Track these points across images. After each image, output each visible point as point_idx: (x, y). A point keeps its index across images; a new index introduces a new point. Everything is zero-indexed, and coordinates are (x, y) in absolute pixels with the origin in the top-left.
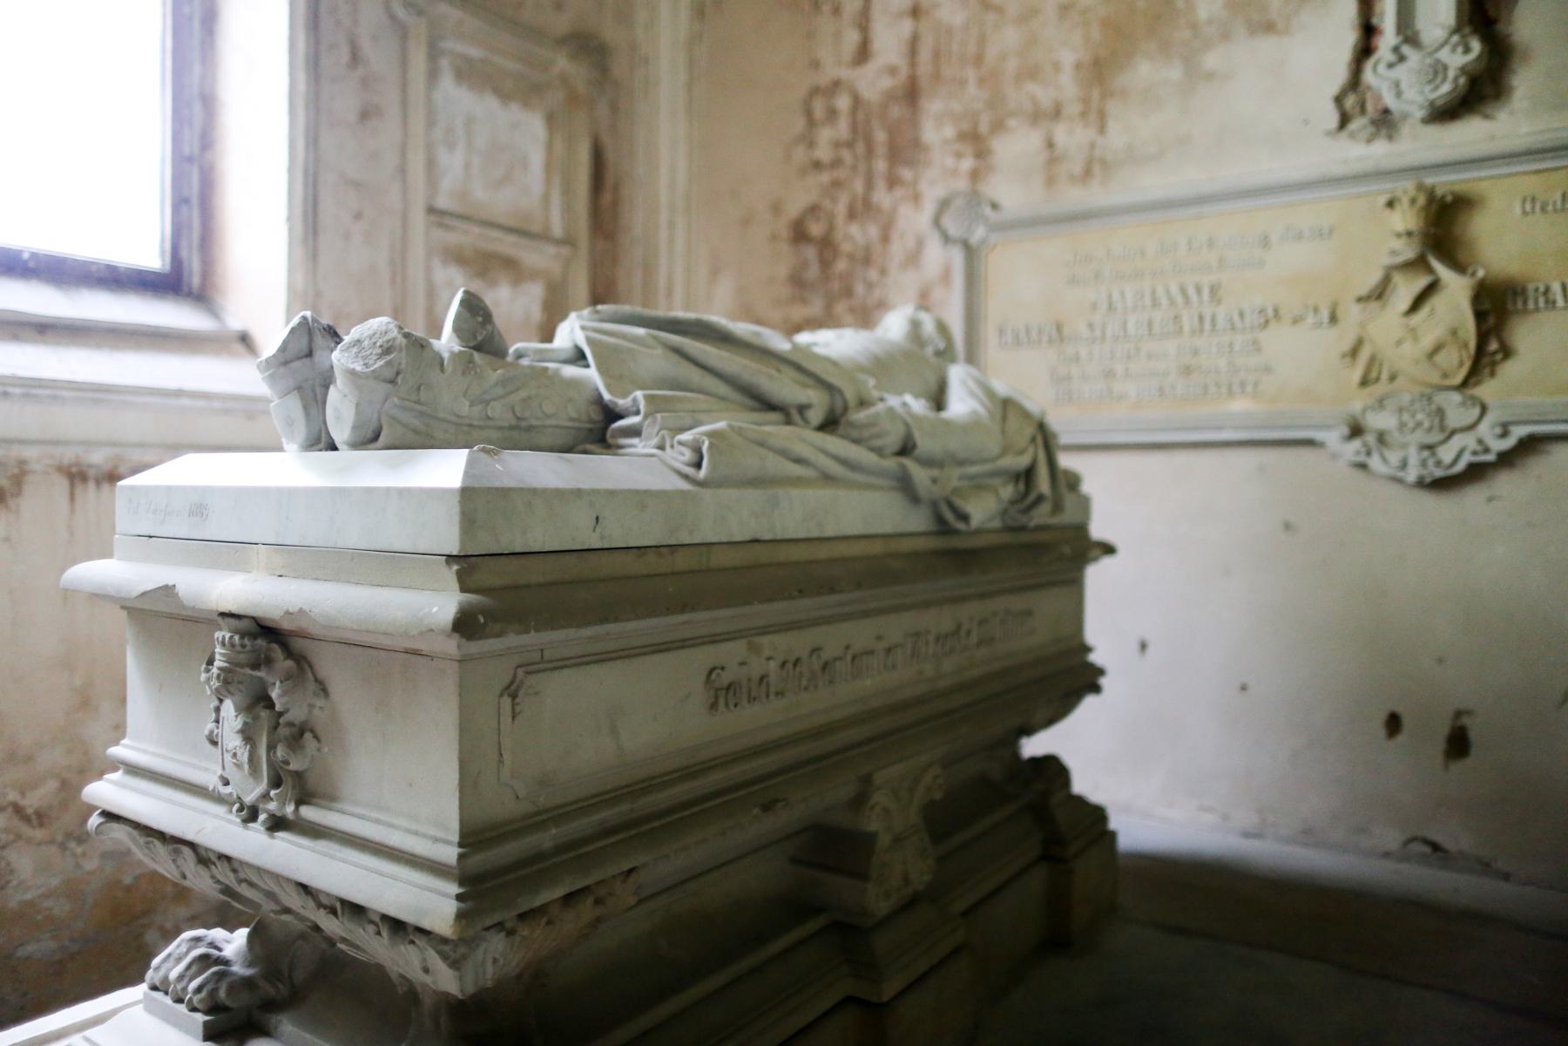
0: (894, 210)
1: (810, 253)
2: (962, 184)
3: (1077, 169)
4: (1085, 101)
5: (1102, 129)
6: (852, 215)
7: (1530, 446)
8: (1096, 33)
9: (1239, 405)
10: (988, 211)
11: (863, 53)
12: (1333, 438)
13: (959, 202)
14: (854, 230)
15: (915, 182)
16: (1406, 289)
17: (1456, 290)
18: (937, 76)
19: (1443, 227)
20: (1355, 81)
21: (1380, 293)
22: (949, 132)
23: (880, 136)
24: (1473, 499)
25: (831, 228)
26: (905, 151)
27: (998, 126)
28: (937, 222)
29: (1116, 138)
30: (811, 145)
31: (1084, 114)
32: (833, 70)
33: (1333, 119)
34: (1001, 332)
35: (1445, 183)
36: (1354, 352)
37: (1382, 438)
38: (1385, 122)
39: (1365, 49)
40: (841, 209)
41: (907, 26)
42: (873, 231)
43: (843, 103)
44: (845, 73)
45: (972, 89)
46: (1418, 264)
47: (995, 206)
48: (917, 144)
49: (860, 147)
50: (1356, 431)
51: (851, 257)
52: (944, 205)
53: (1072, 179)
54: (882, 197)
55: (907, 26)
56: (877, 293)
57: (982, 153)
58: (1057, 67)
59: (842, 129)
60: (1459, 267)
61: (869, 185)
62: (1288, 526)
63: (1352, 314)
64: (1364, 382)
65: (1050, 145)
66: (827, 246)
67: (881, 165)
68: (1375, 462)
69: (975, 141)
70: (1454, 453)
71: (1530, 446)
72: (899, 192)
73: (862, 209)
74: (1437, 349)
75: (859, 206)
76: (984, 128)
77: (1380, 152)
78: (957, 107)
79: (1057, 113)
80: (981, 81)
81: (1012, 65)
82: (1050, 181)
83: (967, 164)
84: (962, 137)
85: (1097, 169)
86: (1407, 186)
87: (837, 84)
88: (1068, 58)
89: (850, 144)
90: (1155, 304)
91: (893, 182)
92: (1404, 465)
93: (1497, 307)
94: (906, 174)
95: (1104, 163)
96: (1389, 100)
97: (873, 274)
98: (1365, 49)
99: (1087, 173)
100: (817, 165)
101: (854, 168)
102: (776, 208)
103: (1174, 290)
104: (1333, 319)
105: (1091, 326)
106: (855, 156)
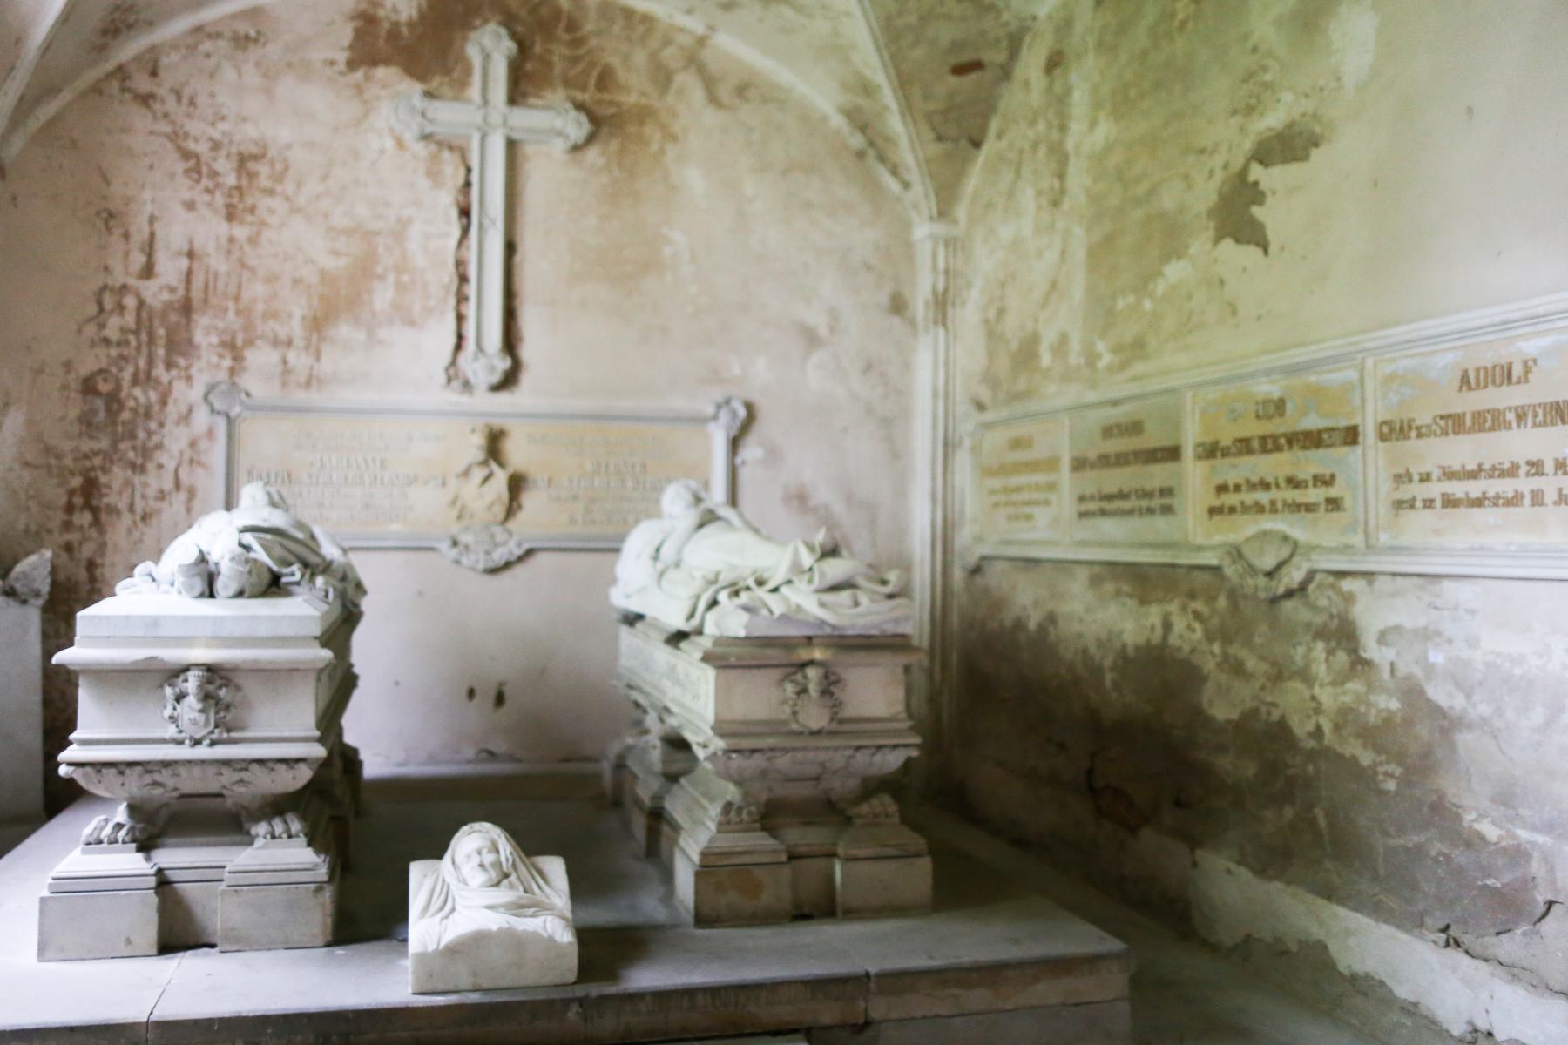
0: (170, 383)
1: (99, 403)
2: (222, 375)
3: (303, 380)
4: (308, 340)
5: (318, 359)
6: (135, 382)
7: (530, 553)
8: (315, 301)
9: (395, 527)
10: (243, 396)
11: (148, 271)
12: (444, 546)
13: (223, 387)
14: (137, 392)
15: (187, 368)
16: (478, 474)
17: (501, 478)
18: (206, 301)
19: (494, 445)
20: (454, 362)
21: (466, 473)
22: (214, 339)
23: (161, 332)
24: (506, 578)
25: (118, 387)
26: (180, 347)
27: (249, 343)
28: (206, 398)
29: (326, 365)
30: (102, 326)
31: (307, 348)
32: (119, 278)
33: (443, 379)
34: (250, 473)
35: (497, 423)
36: (454, 502)
37: (467, 547)
38: (467, 386)
39: (459, 347)
40: (127, 375)
41: (184, 263)
42: (153, 396)
43: (130, 302)
44: (132, 281)
45: (231, 315)
46: (485, 463)
47: (247, 394)
48: (190, 342)
49: (144, 337)
50: (455, 543)
51: (134, 411)
52: (211, 388)
53: (299, 385)
54: (160, 371)
55: (184, 263)
56: (155, 439)
57: (238, 358)
58: (290, 315)
59: (130, 319)
60: (501, 465)
61: (151, 362)
62: (420, 593)
63: (453, 482)
64: (459, 517)
65: (285, 362)
66: (114, 401)
67: (161, 352)
68: (464, 560)
69: (233, 349)
70: (499, 556)
71: (530, 553)
72: (174, 372)
73: (144, 379)
74: (492, 504)
75: (142, 376)
76: (239, 342)
77: (465, 399)
78: (221, 325)
79: (289, 343)
80: (238, 313)
81: (260, 307)
82: (284, 384)
84: (223, 344)
86: (480, 423)
87: (124, 287)
88: (298, 313)
89: (136, 332)
90: (349, 466)
91: (170, 365)
92: (477, 561)
93: (517, 485)
94: (182, 362)
95: (320, 382)
96: (470, 375)
97: (153, 426)
98: (459, 347)
99: (308, 383)
100: (106, 341)
101: (138, 349)
102: (68, 366)
103: (360, 460)
104: (444, 484)
105: (310, 476)
106: (138, 340)
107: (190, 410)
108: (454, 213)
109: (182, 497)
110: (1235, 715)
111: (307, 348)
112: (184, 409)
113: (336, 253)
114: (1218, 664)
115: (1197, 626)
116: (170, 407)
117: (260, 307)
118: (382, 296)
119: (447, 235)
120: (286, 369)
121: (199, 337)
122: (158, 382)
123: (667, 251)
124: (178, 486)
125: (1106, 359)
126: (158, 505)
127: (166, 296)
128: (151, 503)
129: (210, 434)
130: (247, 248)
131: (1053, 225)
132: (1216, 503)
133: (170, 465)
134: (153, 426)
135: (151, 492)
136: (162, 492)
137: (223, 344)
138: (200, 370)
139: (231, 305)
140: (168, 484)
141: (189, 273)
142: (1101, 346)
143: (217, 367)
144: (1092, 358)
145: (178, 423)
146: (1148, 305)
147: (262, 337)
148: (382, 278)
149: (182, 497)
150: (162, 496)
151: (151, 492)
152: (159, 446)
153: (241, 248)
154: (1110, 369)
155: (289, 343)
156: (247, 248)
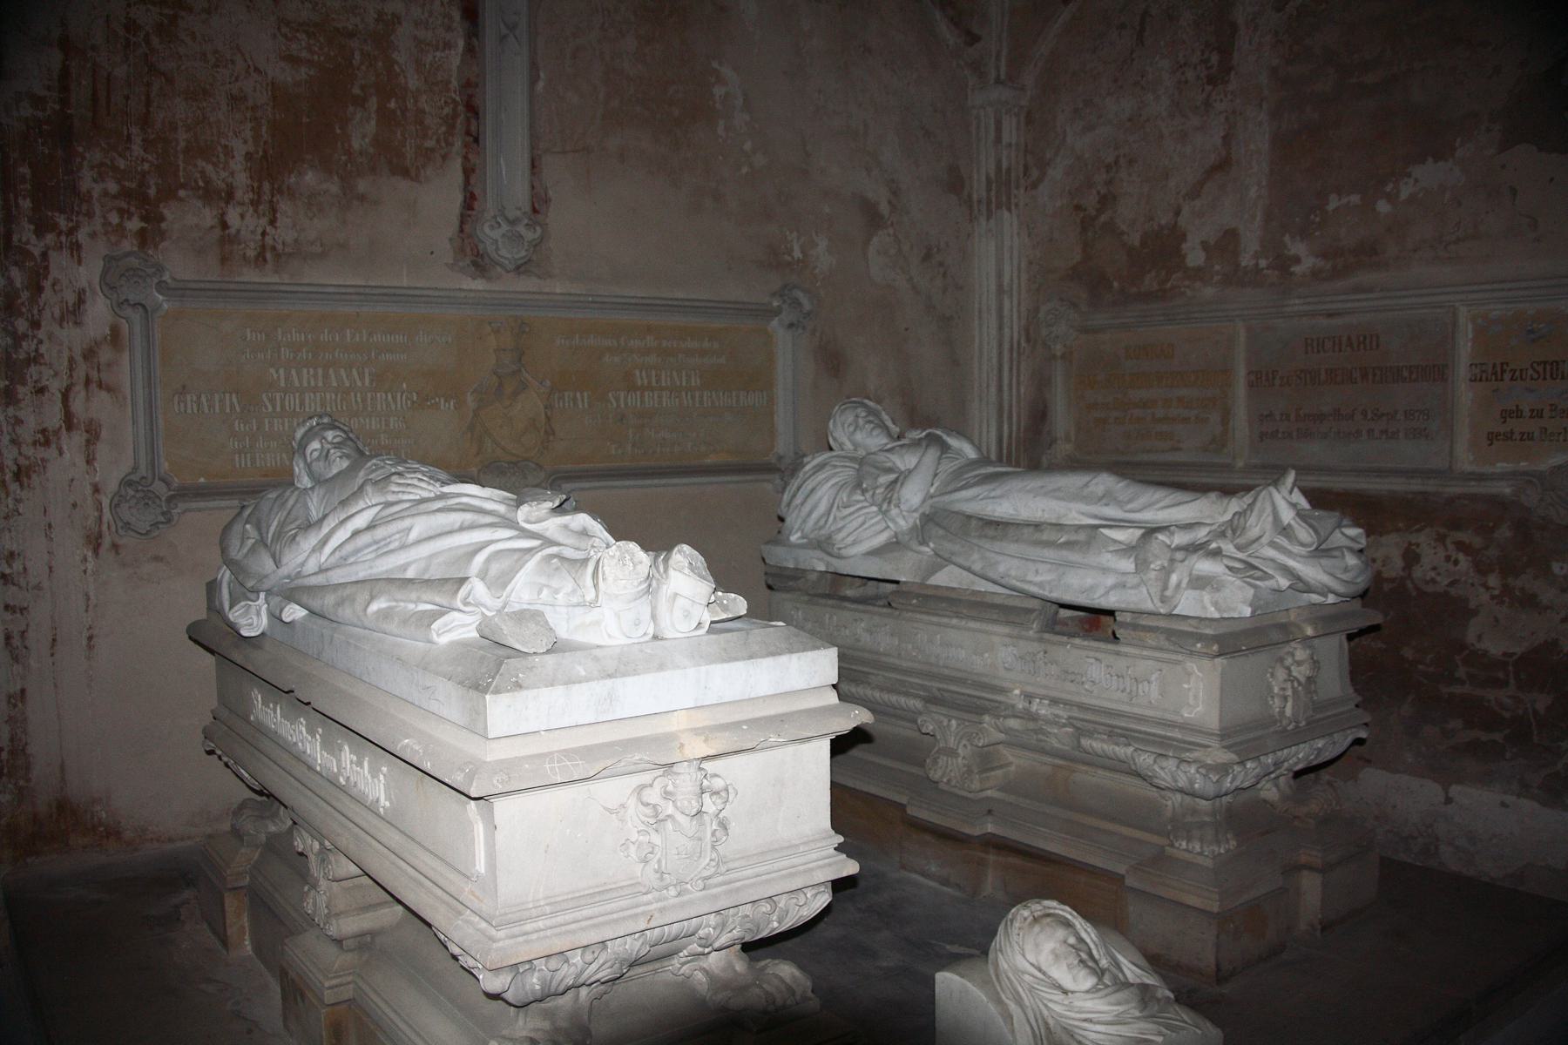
0: (44, 255)
3: (251, 253)
4: (258, 192)
5: (272, 222)
22: (113, 187)
27: (168, 193)
29: (284, 234)
31: (255, 203)
45: (137, 149)
54: (25, 233)
58: (229, 152)
65: (225, 225)
67: (26, 204)
72: (50, 238)
76: (152, 192)
80: (147, 144)
82: (224, 260)
83: (134, 224)
84: (125, 194)
85: (268, 255)
88: (240, 149)
91: (41, 229)
94: (63, 223)
97: (21, 325)
107: (81, 301)
108: (456, 15)
109: (79, 438)
110: (1518, 650)
111: (255, 203)
112: (71, 298)
113: (293, 60)
114: (1493, 597)
115: (1461, 557)
116: (47, 294)
117: (182, 137)
118: (362, 132)
119: (448, 45)
120: (227, 238)
121: (86, 182)
122: (28, 254)
123: (718, 91)
124: (69, 421)
125: (1308, 263)
126: (42, 452)
127: (26, 110)
128: (24, 449)
129: (115, 337)
130: (155, 41)
131: (1207, 104)
132: (1502, 429)
133: (56, 386)
134: (21, 325)
135: (27, 432)
136: (44, 431)
137: (125, 194)
138: (93, 235)
139: (135, 130)
140: (54, 419)
141: (65, 73)
142: (1297, 248)
143: (120, 230)
144: (1283, 263)
145: (61, 321)
146: (1383, 207)
147: (183, 186)
148: (360, 102)
149: (79, 438)
150: (45, 438)
151: (27, 432)
152: (36, 359)
153: (147, 41)
154: (1316, 274)
155: (230, 195)
156: (155, 41)
